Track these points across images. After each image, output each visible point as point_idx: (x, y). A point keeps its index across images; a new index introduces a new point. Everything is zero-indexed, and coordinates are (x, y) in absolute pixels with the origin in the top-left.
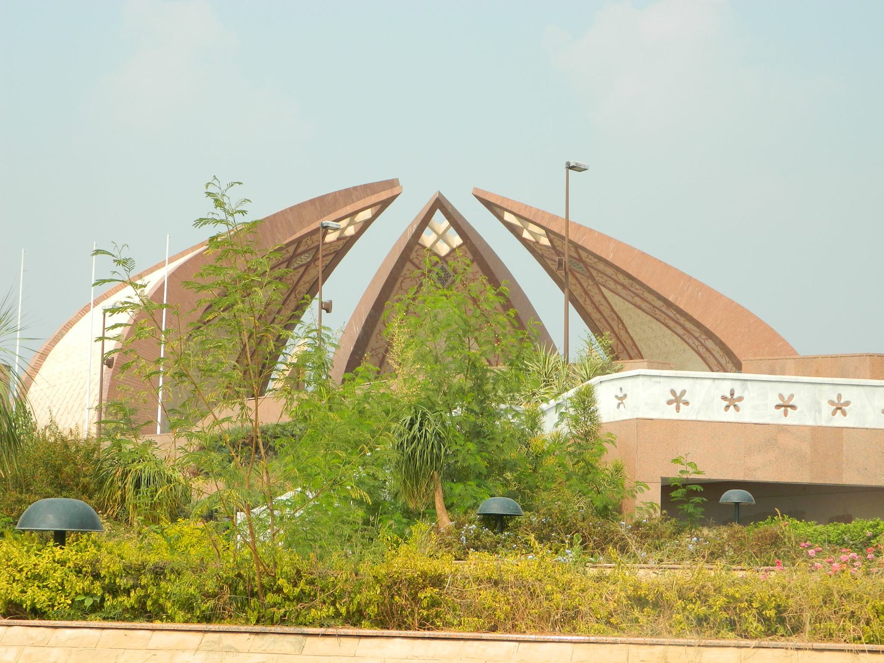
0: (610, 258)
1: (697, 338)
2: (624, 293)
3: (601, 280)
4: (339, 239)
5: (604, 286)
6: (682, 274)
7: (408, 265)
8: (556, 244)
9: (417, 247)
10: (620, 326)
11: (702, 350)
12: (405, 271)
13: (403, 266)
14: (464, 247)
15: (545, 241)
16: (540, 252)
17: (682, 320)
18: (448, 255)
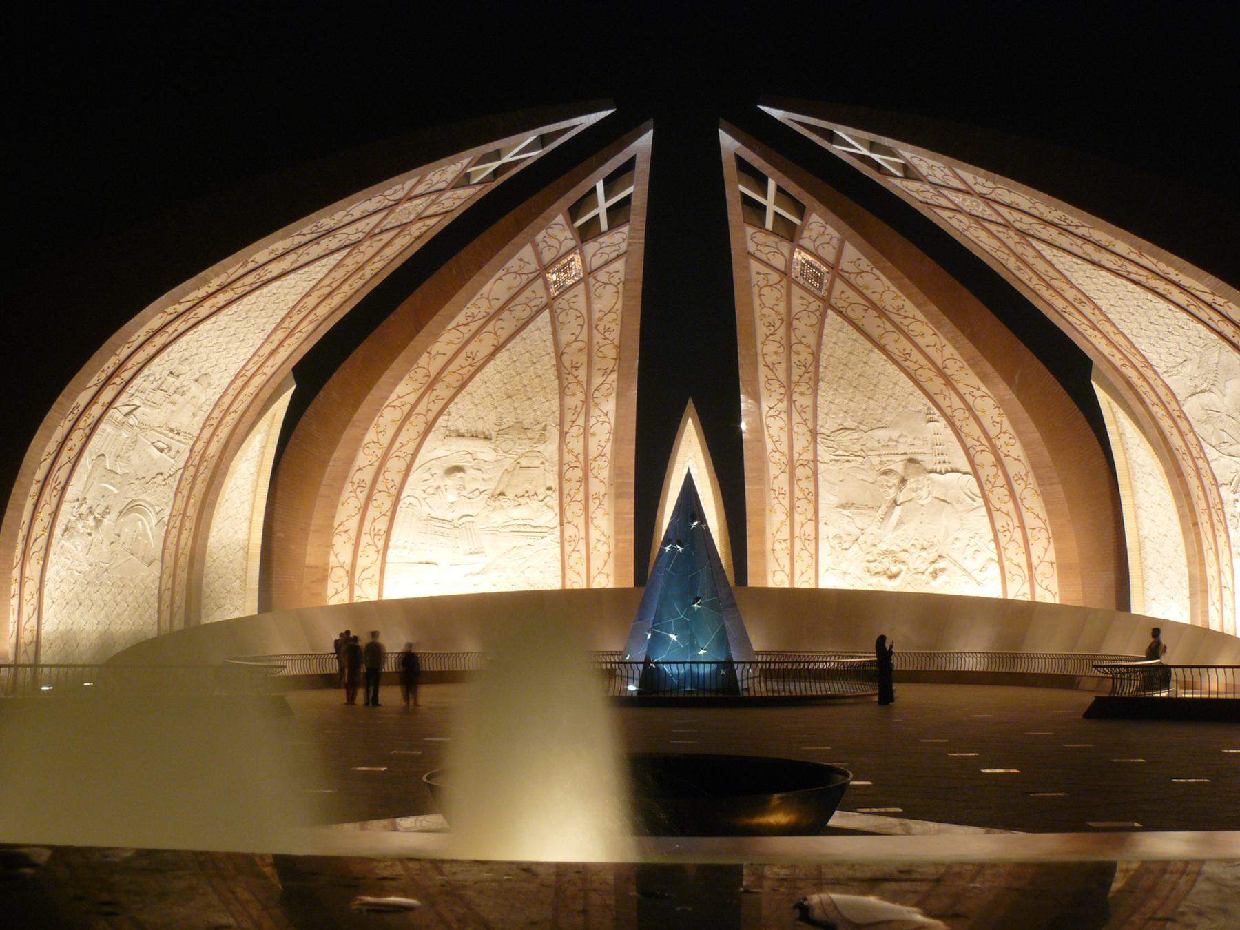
1: (1210, 306)
2: (1064, 241)
3: (1025, 227)
5: (1032, 236)
10: (1096, 312)
12: (755, 278)
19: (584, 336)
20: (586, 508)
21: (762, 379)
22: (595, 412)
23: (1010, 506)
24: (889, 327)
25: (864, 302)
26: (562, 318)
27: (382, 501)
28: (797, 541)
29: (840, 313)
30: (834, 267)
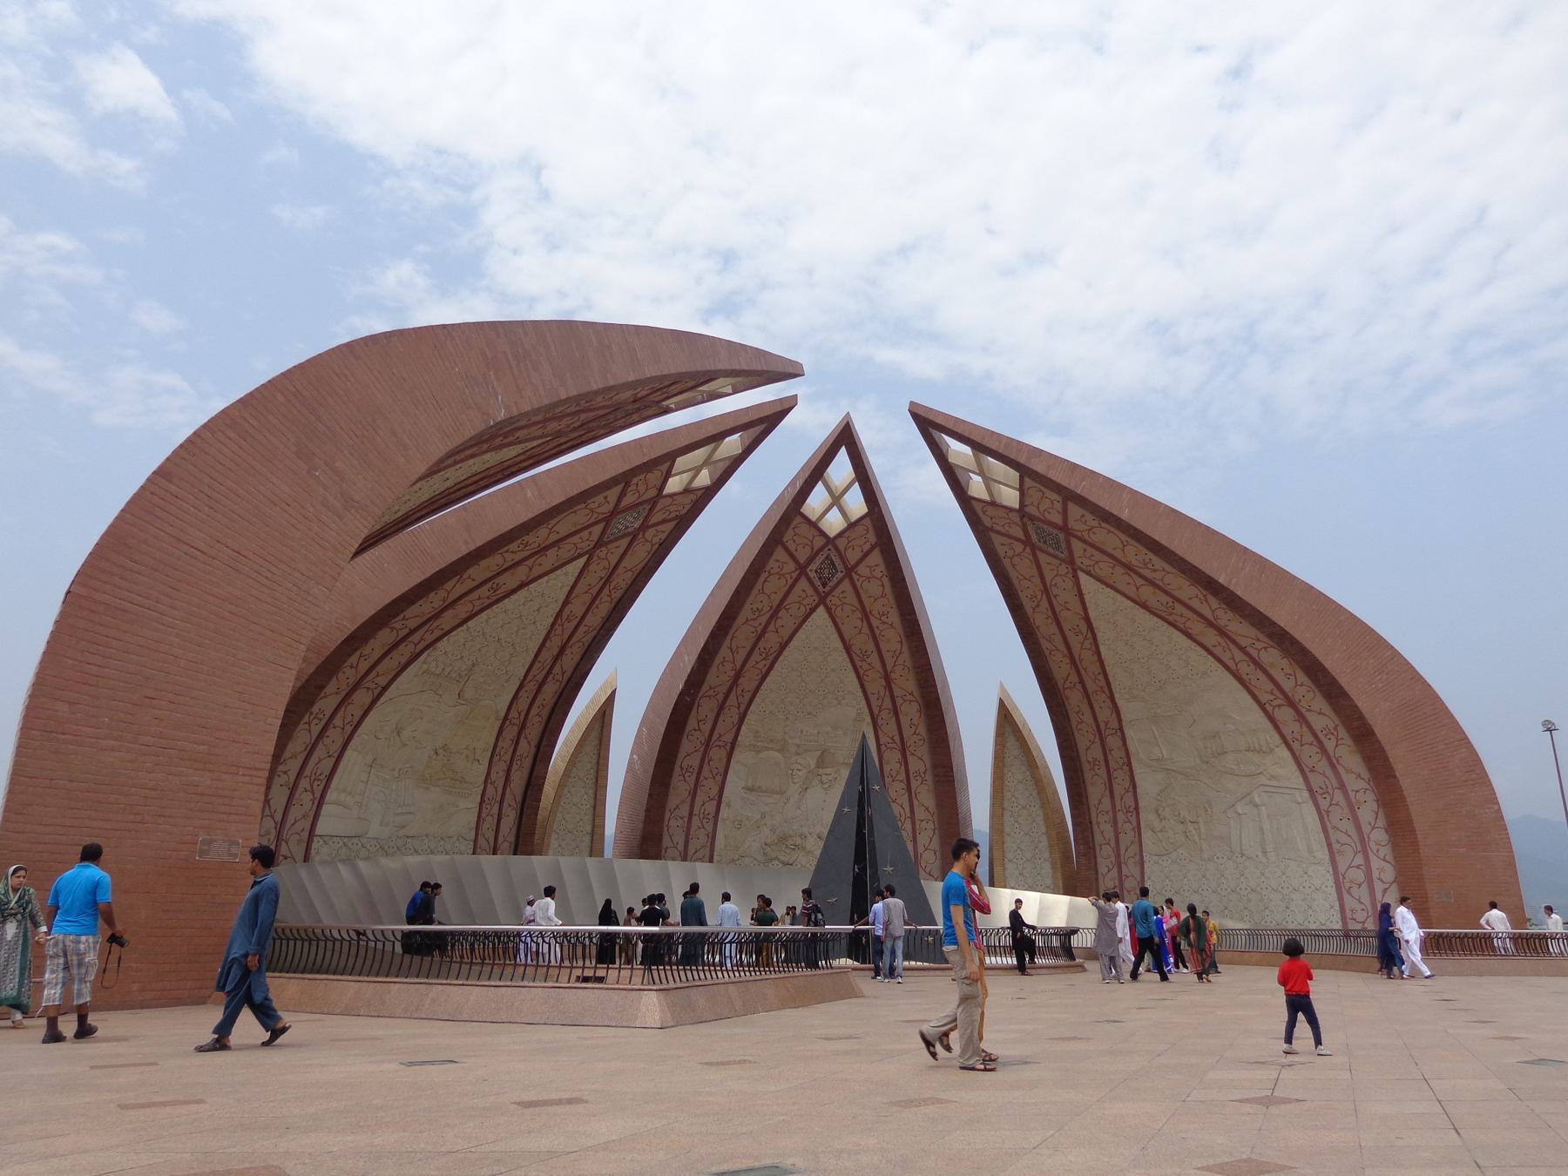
0: (1125, 515)
1: (1242, 649)
4: (687, 491)
5: (1088, 573)
6: (1233, 545)
7: (779, 554)
8: (1028, 501)
9: (798, 519)
10: (1087, 644)
11: (1245, 669)
12: (772, 564)
13: (771, 554)
14: (867, 522)
15: (1010, 497)
16: (987, 522)
17: (1226, 618)
18: (840, 535)
19: (594, 591)
20: (509, 770)
21: (718, 660)
22: (557, 669)
23: (905, 800)
24: (866, 630)
25: (856, 604)
26: (593, 567)
27: (335, 737)
28: (695, 819)
29: (829, 610)
30: (850, 571)
